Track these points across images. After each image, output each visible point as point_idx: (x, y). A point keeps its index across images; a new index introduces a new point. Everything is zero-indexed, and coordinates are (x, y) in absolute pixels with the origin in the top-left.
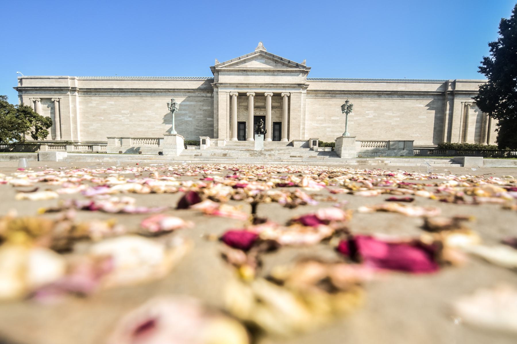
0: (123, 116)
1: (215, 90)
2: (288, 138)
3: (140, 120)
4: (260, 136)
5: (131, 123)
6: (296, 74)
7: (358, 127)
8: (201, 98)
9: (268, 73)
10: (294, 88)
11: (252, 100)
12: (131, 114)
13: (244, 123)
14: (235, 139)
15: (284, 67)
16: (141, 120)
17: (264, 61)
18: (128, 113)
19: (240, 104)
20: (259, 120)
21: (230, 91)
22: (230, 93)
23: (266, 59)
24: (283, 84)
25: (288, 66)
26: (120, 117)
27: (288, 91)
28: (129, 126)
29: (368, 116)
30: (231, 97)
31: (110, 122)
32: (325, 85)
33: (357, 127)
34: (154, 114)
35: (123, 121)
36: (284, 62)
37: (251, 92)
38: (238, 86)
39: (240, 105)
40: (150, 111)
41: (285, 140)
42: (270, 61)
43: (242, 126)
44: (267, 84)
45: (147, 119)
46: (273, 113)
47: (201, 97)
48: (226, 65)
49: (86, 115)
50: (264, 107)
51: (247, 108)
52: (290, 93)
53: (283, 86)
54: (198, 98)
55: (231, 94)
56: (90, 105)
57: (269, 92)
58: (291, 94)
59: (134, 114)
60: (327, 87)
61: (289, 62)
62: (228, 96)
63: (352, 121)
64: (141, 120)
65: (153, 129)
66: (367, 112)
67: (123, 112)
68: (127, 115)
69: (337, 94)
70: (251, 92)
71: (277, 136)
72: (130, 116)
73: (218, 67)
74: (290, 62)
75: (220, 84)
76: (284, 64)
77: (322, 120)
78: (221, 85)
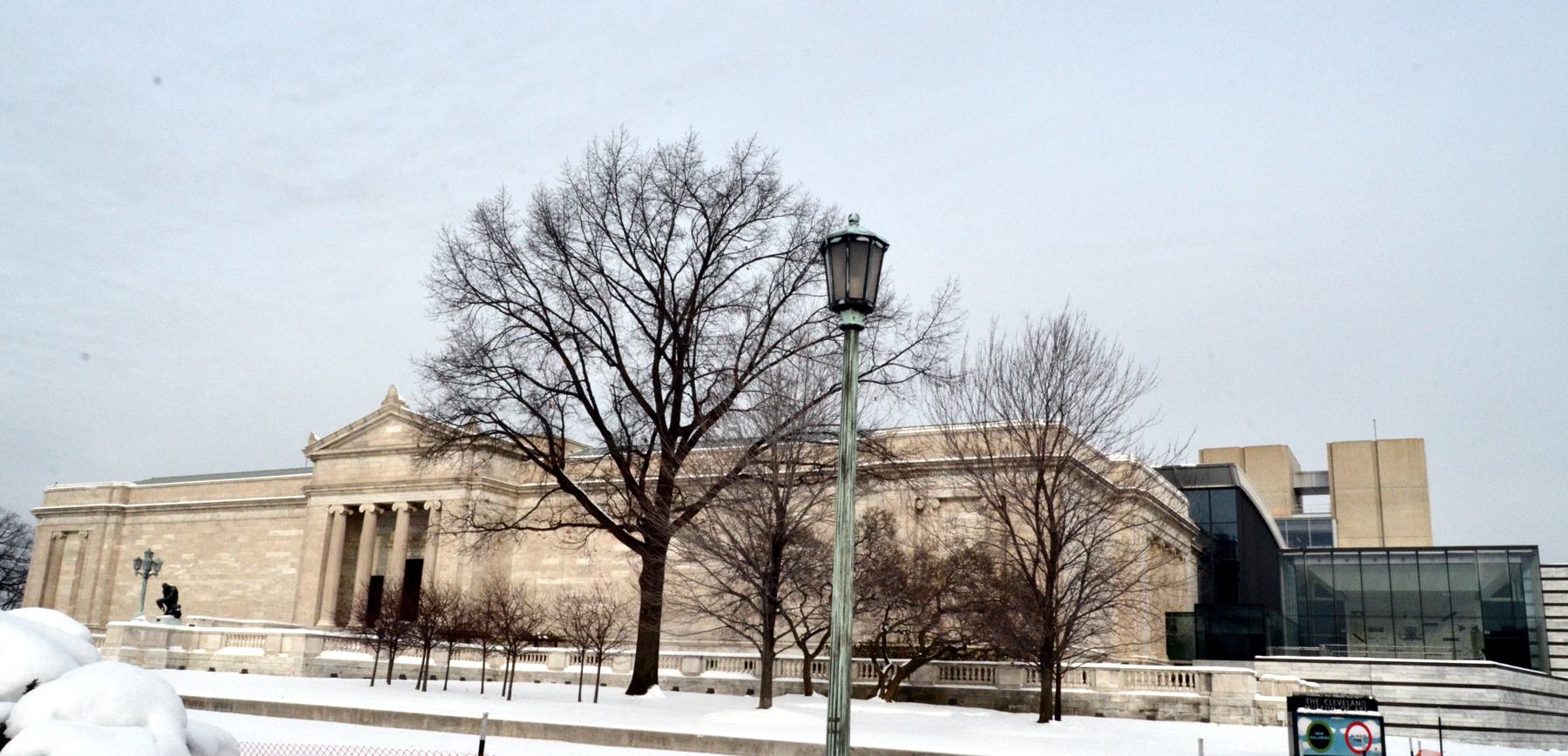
0: (183, 568)
5: (192, 582)
12: (196, 562)
14: (326, 621)
16: (210, 577)
26: (178, 570)
35: (180, 577)
37: (367, 502)
40: (228, 554)
45: (219, 573)
57: (400, 501)
59: (200, 562)
64: (210, 577)
65: (225, 598)
67: (185, 556)
70: (367, 502)
77: (553, 568)
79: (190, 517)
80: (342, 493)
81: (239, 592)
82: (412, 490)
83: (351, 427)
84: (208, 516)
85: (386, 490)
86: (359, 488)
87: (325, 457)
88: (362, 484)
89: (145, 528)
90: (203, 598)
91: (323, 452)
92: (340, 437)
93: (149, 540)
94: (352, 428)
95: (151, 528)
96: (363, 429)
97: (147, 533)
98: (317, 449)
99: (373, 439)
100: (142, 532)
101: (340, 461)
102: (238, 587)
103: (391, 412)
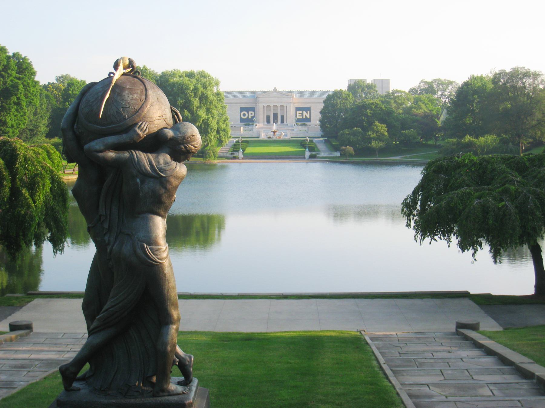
1: (258, 104)
2: (287, 123)
11: (272, 108)
13: (269, 116)
14: (266, 123)
20: (275, 115)
27: (287, 104)
30: (264, 107)
37: (272, 105)
41: (285, 123)
43: (268, 117)
50: (277, 110)
51: (270, 110)
57: (279, 105)
70: (272, 105)
71: (282, 122)
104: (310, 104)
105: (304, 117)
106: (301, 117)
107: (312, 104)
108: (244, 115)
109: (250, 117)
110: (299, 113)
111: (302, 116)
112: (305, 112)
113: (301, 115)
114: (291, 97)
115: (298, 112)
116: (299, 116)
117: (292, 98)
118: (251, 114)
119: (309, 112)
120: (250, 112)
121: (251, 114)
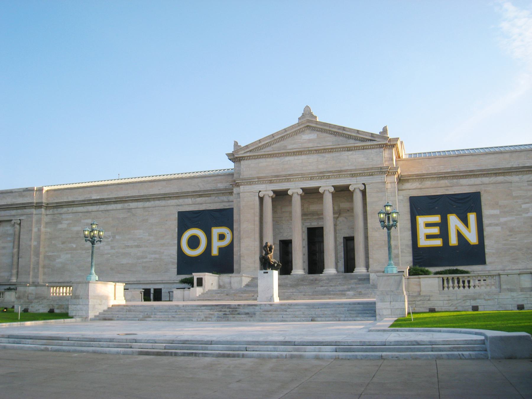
1: (235, 190)
2: (367, 267)
3: (126, 246)
4: (267, 273)
5: (113, 251)
6: (372, 151)
7: (512, 235)
8: (219, 204)
9: (324, 155)
10: (371, 175)
11: (297, 201)
12: (114, 237)
15: (352, 141)
16: (128, 247)
17: (316, 135)
18: (109, 236)
19: (283, 210)
21: (260, 190)
22: (260, 193)
23: (318, 133)
24: (351, 170)
25: (356, 139)
28: (110, 256)
29: (527, 213)
30: (261, 199)
31: (84, 252)
32: (436, 165)
33: (508, 235)
34: (147, 234)
35: (101, 248)
36: (349, 133)
38: (272, 180)
39: (283, 210)
40: (142, 231)
41: (360, 270)
42: (325, 135)
44: (321, 173)
45: (136, 244)
46: (343, 221)
47: (221, 202)
48: (250, 149)
49: (53, 242)
52: (364, 184)
53: (351, 174)
54: (214, 204)
55: (261, 195)
56: (60, 226)
58: (367, 186)
59: (117, 237)
60: (442, 167)
61: (358, 131)
62: (257, 199)
63: (497, 225)
64: (128, 247)
65: (145, 260)
66: (524, 206)
68: (108, 238)
69: (461, 178)
72: (112, 241)
73: (239, 153)
74: (359, 132)
75: (243, 180)
76: (349, 137)
78: (244, 181)
79: (103, 207)
80: (271, 182)
81: (157, 256)
82: (336, 178)
83: (273, 136)
84: (119, 206)
85: (312, 179)
86: (288, 178)
87: (249, 158)
88: (290, 175)
89: (64, 216)
90: (124, 261)
91: (248, 154)
92: (263, 143)
93: (68, 224)
94: (274, 137)
95: (70, 216)
96: (282, 137)
97: (67, 220)
98: (243, 152)
99: (291, 145)
100: (62, 219)
101: (261, 160)
102: (155, 252)
103: (308, 124)
104: (478, 181)
105: (453, 241)
106: (438, 242)
107: (486, 180)
108: (194, 242)
109: (215, 252)
110: (428, 225)
111: (444, 234)
112: (453, 221)
113: (435, 231)
114: (381, 146)
115: (421, 220)
116: (429, 237)
117: (386, 153)
118: (222, 237)
119: (472, 217)
120: (216, 231)
121: (222, 237)
